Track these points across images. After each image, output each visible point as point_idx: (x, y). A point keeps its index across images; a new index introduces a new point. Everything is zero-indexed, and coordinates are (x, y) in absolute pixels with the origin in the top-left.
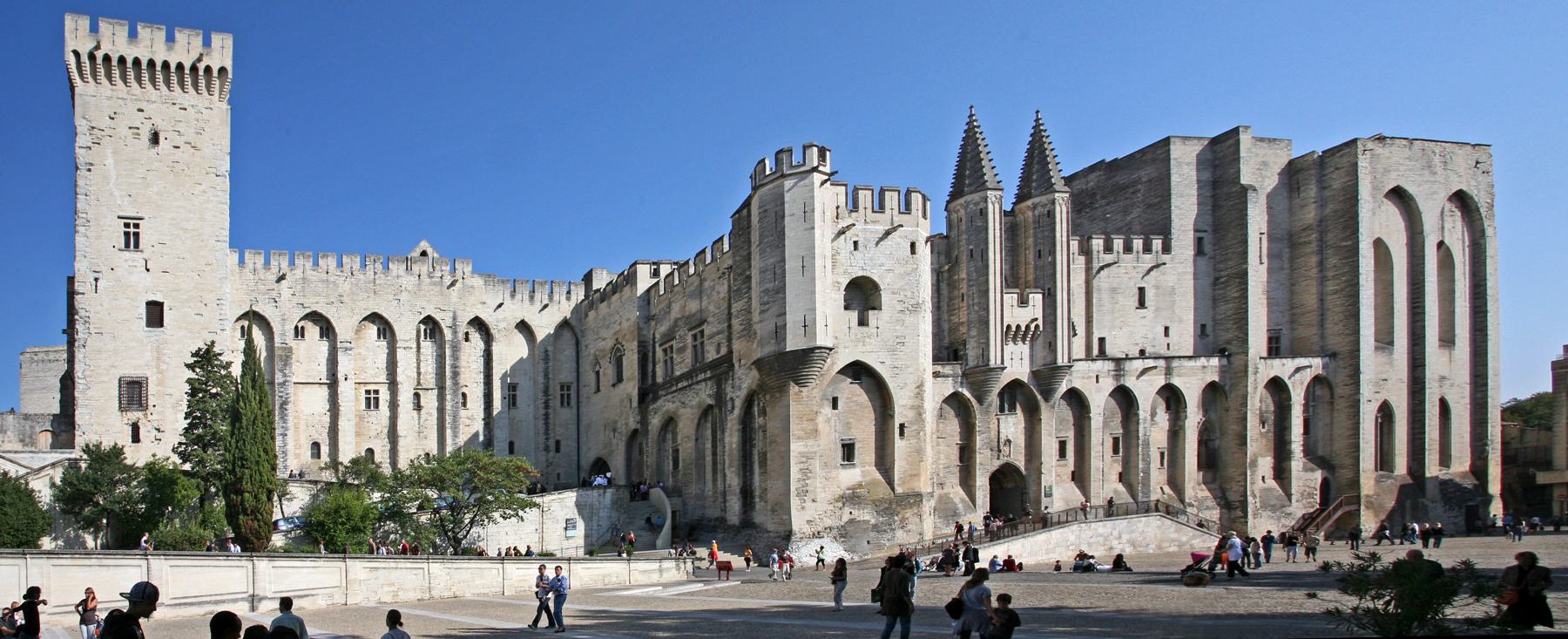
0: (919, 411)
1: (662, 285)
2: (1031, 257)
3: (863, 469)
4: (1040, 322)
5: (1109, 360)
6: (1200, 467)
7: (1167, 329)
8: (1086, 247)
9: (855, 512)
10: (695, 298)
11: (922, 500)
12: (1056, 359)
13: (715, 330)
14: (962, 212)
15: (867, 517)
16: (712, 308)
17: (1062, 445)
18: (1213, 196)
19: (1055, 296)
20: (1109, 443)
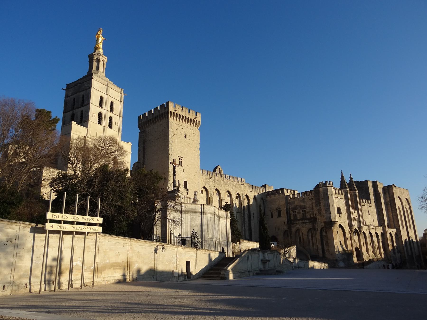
6: (383, 251)
9: (345, 256)
13: (309, 211)
15: (346, 257)
16: (308, 206)
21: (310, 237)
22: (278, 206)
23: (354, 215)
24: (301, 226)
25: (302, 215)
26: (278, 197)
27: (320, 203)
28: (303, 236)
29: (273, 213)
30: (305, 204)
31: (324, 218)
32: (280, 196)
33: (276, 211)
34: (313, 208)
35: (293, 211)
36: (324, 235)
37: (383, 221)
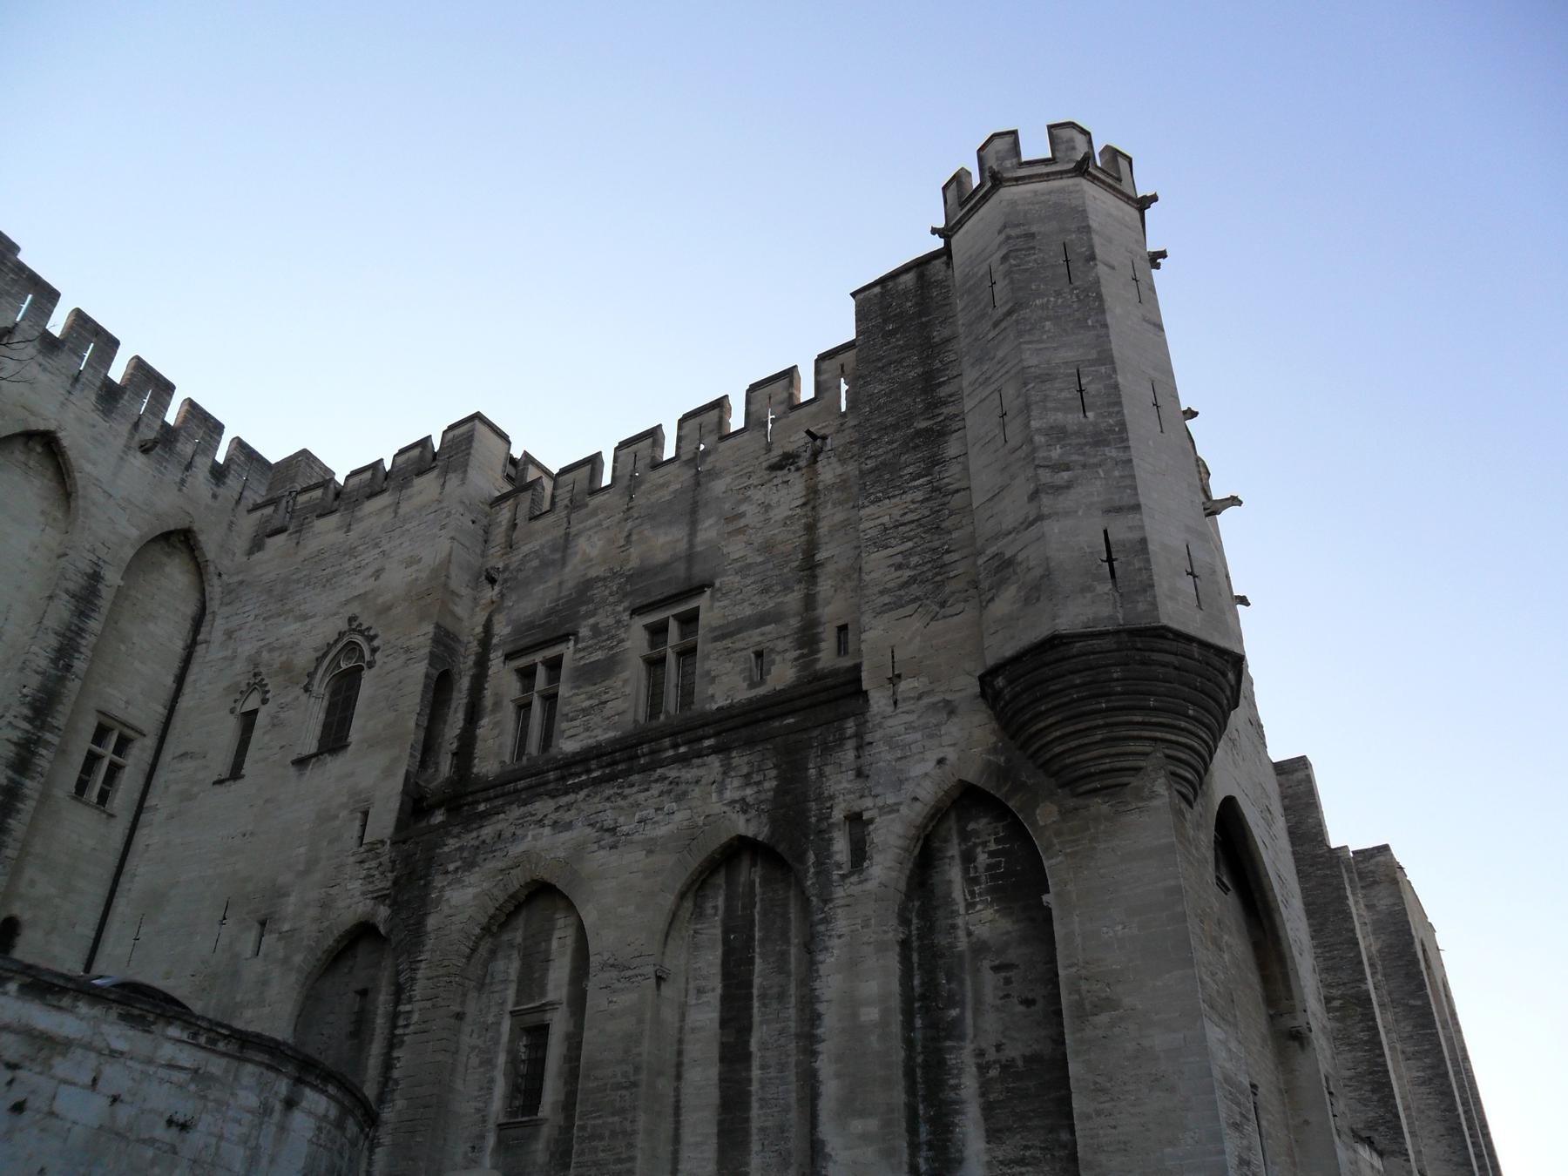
16: (736, 549)
21: (706, 1016)
24: (581, 832)
26: (387, 517)
27: (937, 436)
28: (578, 1002)
29: (260, 716)
31: (1005, 603)
32: (405, 508)
33: (307, 689)
34: (820, 557)
35: (522, 662)
36: (980, 948)
37: (1375, 1097)
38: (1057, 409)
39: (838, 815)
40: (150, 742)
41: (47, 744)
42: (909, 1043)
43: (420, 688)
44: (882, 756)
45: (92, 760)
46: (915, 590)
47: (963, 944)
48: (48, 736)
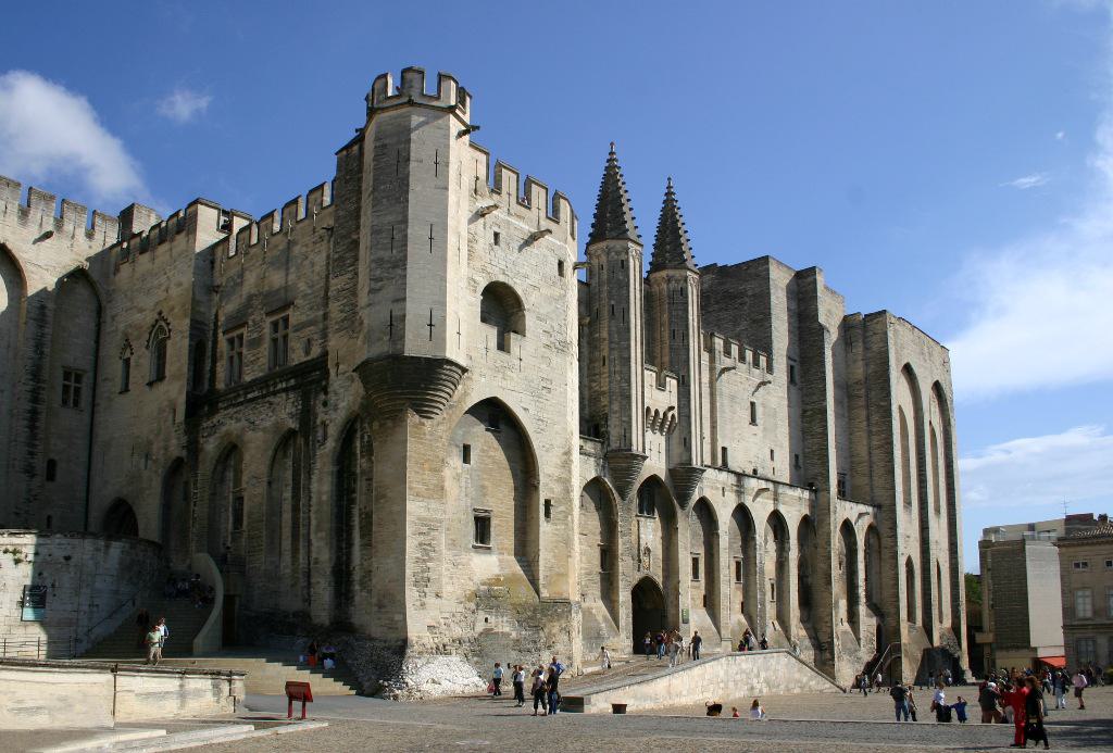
0: (566, 483)
1: (233, 242)
2: (666, 334)
3: (501, 557)
4: (675, 412)
5: (732, 472)
7: (772, 451)
8: (709, 345)
9: (492, 619)
10: (279, 268)
11: (570, 611)
12: (691, 459)
13: (304, 318)
14: (604, 259)
16: (302, 286)
17: (695, 561)
18: (799, 328)
19: (689, 386)
20: (733, 567)
21: (288, 494)
22: (160, 313)
23: (652, 393)
24: (244, 423)
25: (266, 353)
27: (356, 243)
30: (292, 277)
35: (230, 335)
38: (381, 249)
39: (318, 422)
40: (91, 374)
41: (44, 389)
42: (339, 507)
43: (187, 352)
44: (332, 398)
45: (66, 389)
46: (346, 324)
47: (358, 471)
48: (43, 385)
